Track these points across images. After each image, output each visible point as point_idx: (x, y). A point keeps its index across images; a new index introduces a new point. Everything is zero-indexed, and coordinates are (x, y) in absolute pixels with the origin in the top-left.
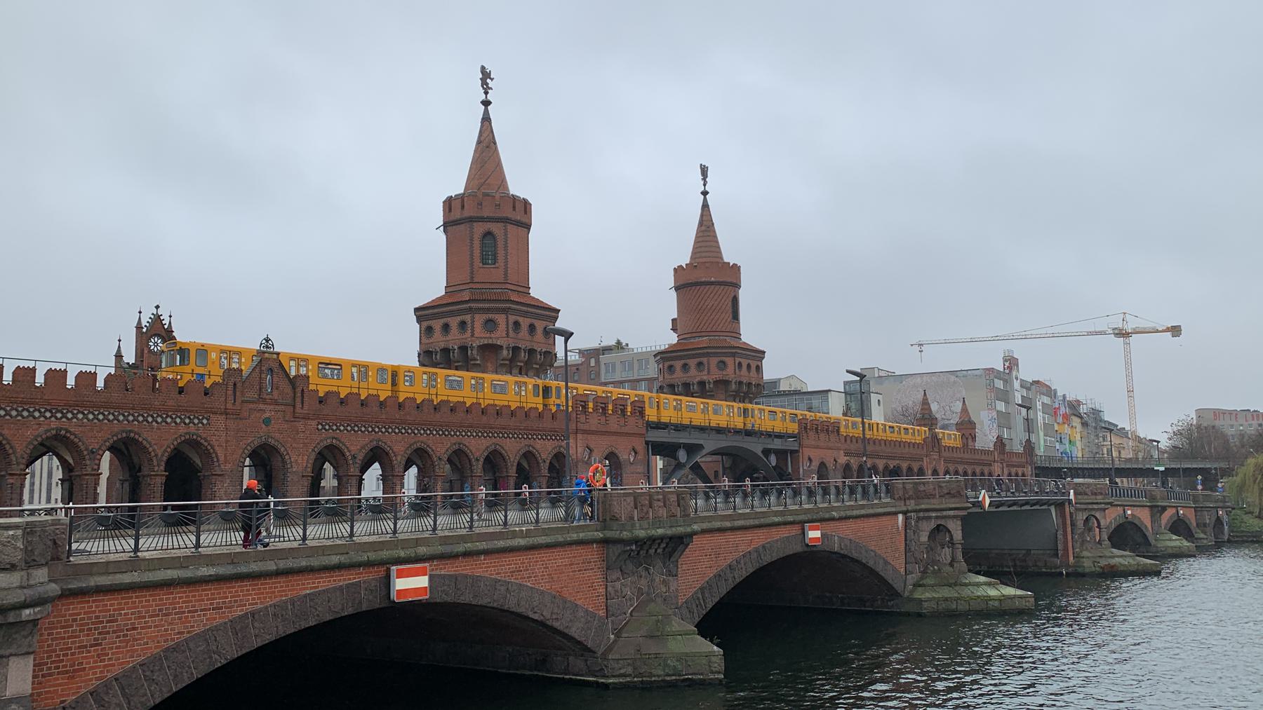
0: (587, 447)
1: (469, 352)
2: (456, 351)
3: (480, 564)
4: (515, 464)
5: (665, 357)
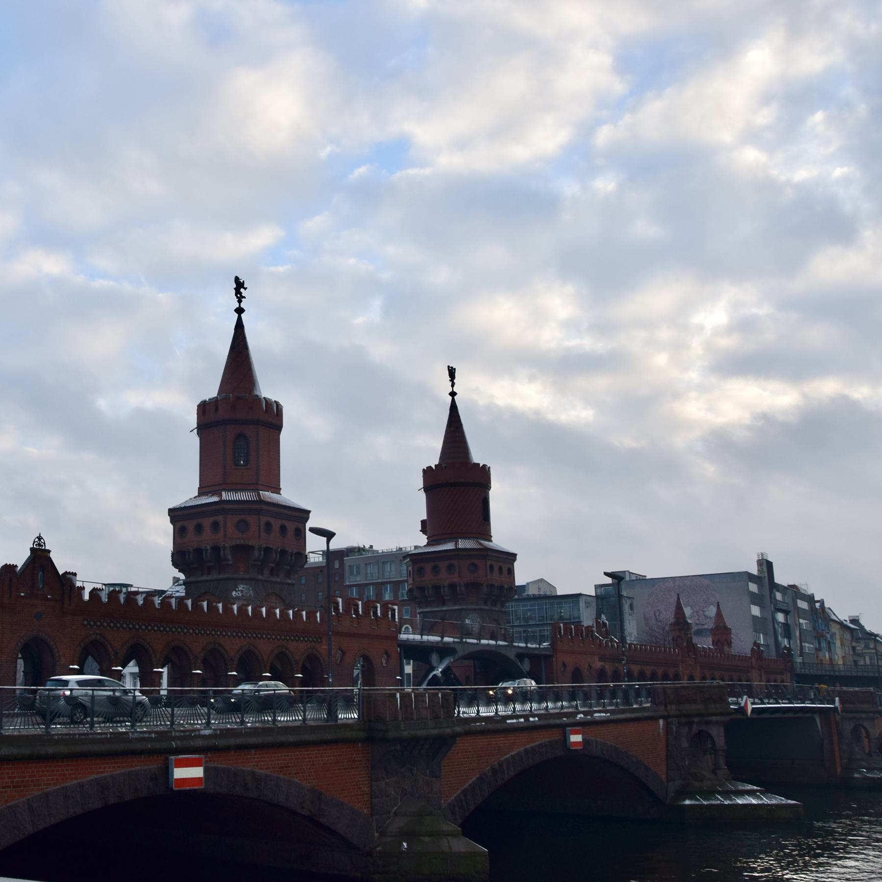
0: (340, 649)
1: (222, 552)
2: (209, 552)
3: (250, 758)
4: (269, 665)
5: (416, 559)
